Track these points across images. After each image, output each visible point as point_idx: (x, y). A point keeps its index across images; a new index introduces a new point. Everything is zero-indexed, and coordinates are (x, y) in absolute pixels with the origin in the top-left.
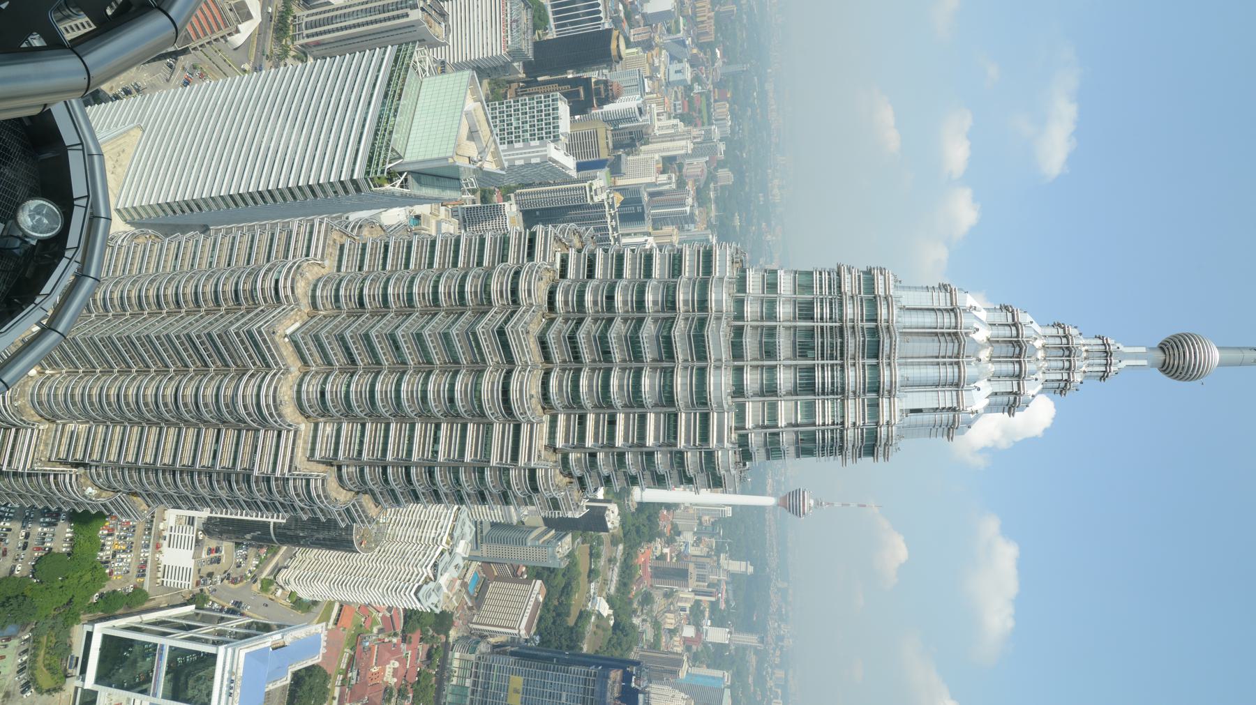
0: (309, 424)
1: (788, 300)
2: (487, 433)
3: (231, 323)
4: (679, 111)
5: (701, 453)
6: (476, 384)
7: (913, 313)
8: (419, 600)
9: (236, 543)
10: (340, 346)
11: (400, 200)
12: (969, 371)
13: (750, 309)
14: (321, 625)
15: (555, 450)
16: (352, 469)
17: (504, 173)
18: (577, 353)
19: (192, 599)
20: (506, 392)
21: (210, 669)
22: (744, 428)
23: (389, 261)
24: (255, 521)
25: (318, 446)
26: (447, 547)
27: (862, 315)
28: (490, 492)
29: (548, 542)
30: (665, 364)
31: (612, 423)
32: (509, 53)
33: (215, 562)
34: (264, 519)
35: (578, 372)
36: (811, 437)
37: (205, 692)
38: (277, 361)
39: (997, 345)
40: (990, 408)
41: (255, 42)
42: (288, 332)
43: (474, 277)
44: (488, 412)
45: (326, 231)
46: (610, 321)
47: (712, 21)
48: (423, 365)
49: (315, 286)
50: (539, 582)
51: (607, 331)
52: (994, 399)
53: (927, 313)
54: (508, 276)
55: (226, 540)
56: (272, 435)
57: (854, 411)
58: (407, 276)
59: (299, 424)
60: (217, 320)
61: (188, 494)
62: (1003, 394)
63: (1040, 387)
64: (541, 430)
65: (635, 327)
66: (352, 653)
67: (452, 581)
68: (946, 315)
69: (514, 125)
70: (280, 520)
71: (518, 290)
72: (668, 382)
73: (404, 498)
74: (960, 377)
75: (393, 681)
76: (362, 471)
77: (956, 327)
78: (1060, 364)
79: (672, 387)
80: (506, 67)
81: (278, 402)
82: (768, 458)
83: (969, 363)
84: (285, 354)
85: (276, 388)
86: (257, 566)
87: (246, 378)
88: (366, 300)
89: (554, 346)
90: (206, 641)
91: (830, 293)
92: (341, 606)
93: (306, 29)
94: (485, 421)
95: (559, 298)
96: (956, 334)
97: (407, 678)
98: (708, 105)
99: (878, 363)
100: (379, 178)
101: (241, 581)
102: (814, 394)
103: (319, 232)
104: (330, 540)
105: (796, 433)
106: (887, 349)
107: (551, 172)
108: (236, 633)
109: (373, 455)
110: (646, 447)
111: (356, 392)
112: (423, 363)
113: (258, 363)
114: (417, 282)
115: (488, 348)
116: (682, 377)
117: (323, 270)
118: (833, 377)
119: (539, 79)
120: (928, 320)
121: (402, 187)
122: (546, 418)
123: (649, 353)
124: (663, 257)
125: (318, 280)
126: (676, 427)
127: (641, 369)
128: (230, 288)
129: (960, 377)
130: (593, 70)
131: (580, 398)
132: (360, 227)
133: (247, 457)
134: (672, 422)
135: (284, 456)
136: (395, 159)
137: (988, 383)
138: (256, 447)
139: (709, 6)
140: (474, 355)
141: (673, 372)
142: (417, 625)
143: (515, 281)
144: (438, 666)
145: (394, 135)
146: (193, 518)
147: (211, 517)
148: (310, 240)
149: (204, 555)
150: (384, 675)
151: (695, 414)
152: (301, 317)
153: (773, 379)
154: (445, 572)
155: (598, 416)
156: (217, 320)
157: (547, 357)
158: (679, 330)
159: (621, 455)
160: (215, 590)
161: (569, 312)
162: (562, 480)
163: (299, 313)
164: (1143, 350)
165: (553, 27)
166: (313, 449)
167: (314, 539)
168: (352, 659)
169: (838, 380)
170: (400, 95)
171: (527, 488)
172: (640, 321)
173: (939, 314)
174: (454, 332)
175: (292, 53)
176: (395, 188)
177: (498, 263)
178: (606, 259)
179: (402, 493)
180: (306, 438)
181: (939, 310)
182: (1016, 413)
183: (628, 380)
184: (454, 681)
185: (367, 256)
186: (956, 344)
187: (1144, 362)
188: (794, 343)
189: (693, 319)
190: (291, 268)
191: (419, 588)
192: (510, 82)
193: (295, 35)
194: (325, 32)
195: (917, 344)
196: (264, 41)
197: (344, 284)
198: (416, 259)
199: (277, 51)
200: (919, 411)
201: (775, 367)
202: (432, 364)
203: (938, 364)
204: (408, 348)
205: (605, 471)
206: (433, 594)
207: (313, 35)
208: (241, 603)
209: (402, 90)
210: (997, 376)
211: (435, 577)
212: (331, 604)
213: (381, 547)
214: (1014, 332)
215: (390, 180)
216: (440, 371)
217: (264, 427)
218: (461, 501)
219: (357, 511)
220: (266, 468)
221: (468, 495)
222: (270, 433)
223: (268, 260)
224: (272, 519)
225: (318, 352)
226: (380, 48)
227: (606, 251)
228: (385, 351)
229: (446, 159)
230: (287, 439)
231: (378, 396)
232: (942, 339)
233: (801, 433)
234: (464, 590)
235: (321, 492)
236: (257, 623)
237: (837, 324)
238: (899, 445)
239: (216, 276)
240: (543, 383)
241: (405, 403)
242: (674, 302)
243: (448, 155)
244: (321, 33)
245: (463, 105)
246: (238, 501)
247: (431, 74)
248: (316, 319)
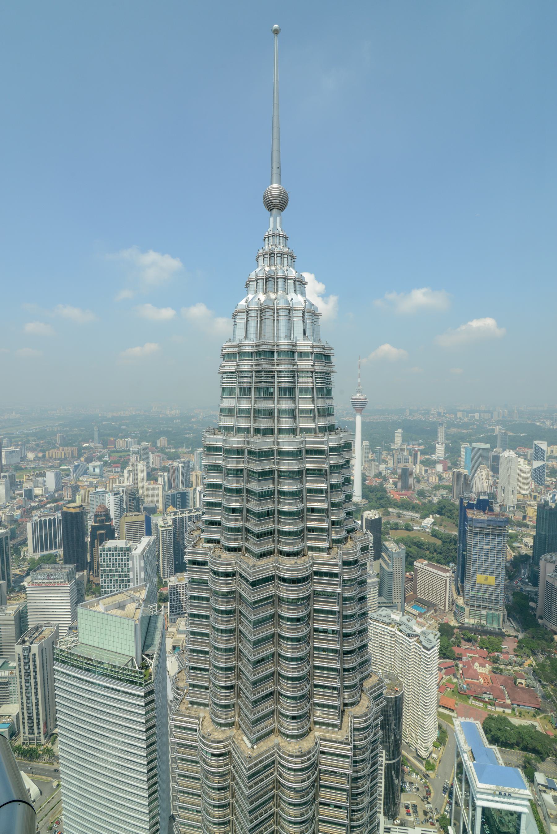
0: (315, 729)
1: (239, 402)
2: (320, 595)
3: (242, 793)
5: (330, 455)
6: (288, 602)
7: (248, 332)
8: (433, 647)
9: (401, 792)
10: (260, 704)
11: (161, 660)
12: (282, 304)
13: (243, 424)
14: (455, 722)
15: (330, 548)
16: (346, 695)
17: (148, 585)
18: (268, 533)
19: (444, 829)
20: (293, 581)
21: (493, 812)
22: (315, 429)
23: (202, 666)
24: (385, 776)
25: (331, 721)
26: (396, 628)
27: (249, 360)
28: (359, 594)
29: (389, 557)
30: (276, 476)
31: (312, 510)
32: (69, 581)
33: (416, 810)
34: (383, 768)
35: (280, 532)
36: (320, 390)
37: (510, 817)
38: (271, 754)
39: (268, 290)
40: (303, 294)
41: (38, 776)
42: (250, 745)
43: (216, 603)
44: (306, 594)
45: (179, 715)
46: (248, 511)
48: (275, 641)
49: (218, 724)
50: (415, 563)
51: (255, 513)
52: (297, 292)
53: (249, 325)
54: (217, 579)
55: (400, 800)
56: (324, 759)
57: (304, 365)
58: (213, 652)
59: (315, 737)
60: (240, 806)
61: (367, 830)
62: (295, 287)
63: (291, 268)
64: (318, 557)
65: (252, 495)
66: (472, 698)
67: (419, 624)
68: (250, 315)
69: (117, 578)
70: (384, 755)
71: (226, 572)
72: (287, 474)
73: (364, 656)
74: (285, 309)
75: (488, 667)
76: (346, 687)
77: (257, 310)
78: (279, 258)
79: (290, 472)
80: (78, 584)
81: (300, 754)
82: (333, 415)
83: (278, 304)
84: (265, 748)
85: (290, 756)
86: (417, 774)
87: (282, 781)
88: (229, 684)
89: (264, 548)
90: (474, 816)
91: (235, 378)
92: (440, 706)
93: (34, 734)
94: (312, 596)
95: (232, 544)
96: (261, 310)
97: (485, 657)
99: (277, 352)
100: (145, 676)
101: (428, 787)
102: (295, 388)
103: (180, 721)
104: (396, 715)
105: (318, 398)
106: (269, 347)
107: (152, 550)
108: (465, 791)
109: (336, 679)
110: (327, 489)
111: (293, 691)
112: (273, 640)
113: (272, 770)
114: (218, 645)
115: (263, 593)
116: (284, 465)
117: (207, 718)
118: (285, 377)
119: (89, 560)
120: (252, 325)
121: (152, 658)
122: (310, 553)
123: (268, 486)
124: (209, 477)
125: (214, 721)
126: (315, 470)
127: (279, 491)
128: (216, 795)
129: (285, 309)
130: (87, 524)
131: (297, 531)
132: (178, 689)
133: (340, 780)
134: (312, 472)
135: (338, 748)
136: (133, 663)
137: (289, 295)
138: (332, 772)
140: (268, 603)
141: (281, 471)
142: (449, 649)
143: (220, 574)
144: (475, 634)
145: (116, 664)
146: (385, 828)
147: (384, 813)
148: (185, 728)
149: (411, 819)
150: (485, 674)
151: (307, 458)
152: (239, 735)
153: (285, 411)
154: (412, 628)
155: (308, 520)
156: (240, 806)
157: (270, 553)
158: (255, 467)
159: (333, 505)
160: (436, 809)
161: (242, 538)
162: (350, 544)
163: (236, 737)
164: (271, 219)
165: (56, 551)
166: (333, 725)
167: (395, 728)
168: (476, 698)
169: (287, 374)
170: (89, 659)
171: (355, 567)
172: (248, 491)
173: (249, 319)
174: (252, 618)
175: (50, 746)
176: (152, 663)
177: (208, 586)
178: (208, 513)
179: (362, 657)
180: (325, 731)
181: (247, 319)
182: (306, 281)
183: (286, 499)
184: (483, 622)
185: (199, 683)
186: (267, 310)
187: (278, 218)
188: (264, 398)
189: (248, 458)
190: (204, 743)
191: (424, 647)
192: (89, 581)
193: (37, 743)
194: (38, 719)
195: (267, 331)
196: (37, 769)
197: (217, 701)
198: (202, 646)
199: (46, 758)
200: (304, 331)
201: (278, 409)
202: (274, 634)
203: (278, 320)
204: (263, 652)
205: (343, 515)
206: (428, 637)
207: (39, 729)
208: (444, 787)
209: (85, 658)
210: (285, 290)
211: (416, 636)
212: (440, 715)
213: (398, 676)
214: (261, 281)
215: (147, 667)
216: (279, 628)
217: (317, 765)
218: (365, 614)
219: (375, 691)
220: (347, 763)
221: (361, 609)
222: (322, 760)
223: (197, 762)
224: (383, 761)
225: (264, 721)
226: (54, 675)
227: (203, 513)
228: (264, 669)
229: (136, 625)
230: (326, 746)
231: (295, 675)
232: (264, 317)
233: (317, 395)
234: (424, 616)
235: (362, 719)
236: (457, 774)
237: (254, 374)
238: (324, 342)
239: (207, 807)
240: (287, 556)
241: (300, 654)
242: (238, 470)
243: (133, 624)
244: (38, 722)
245: (100, 613)
246: (371, 788)
247: (77, 636)
248: (241, 723)
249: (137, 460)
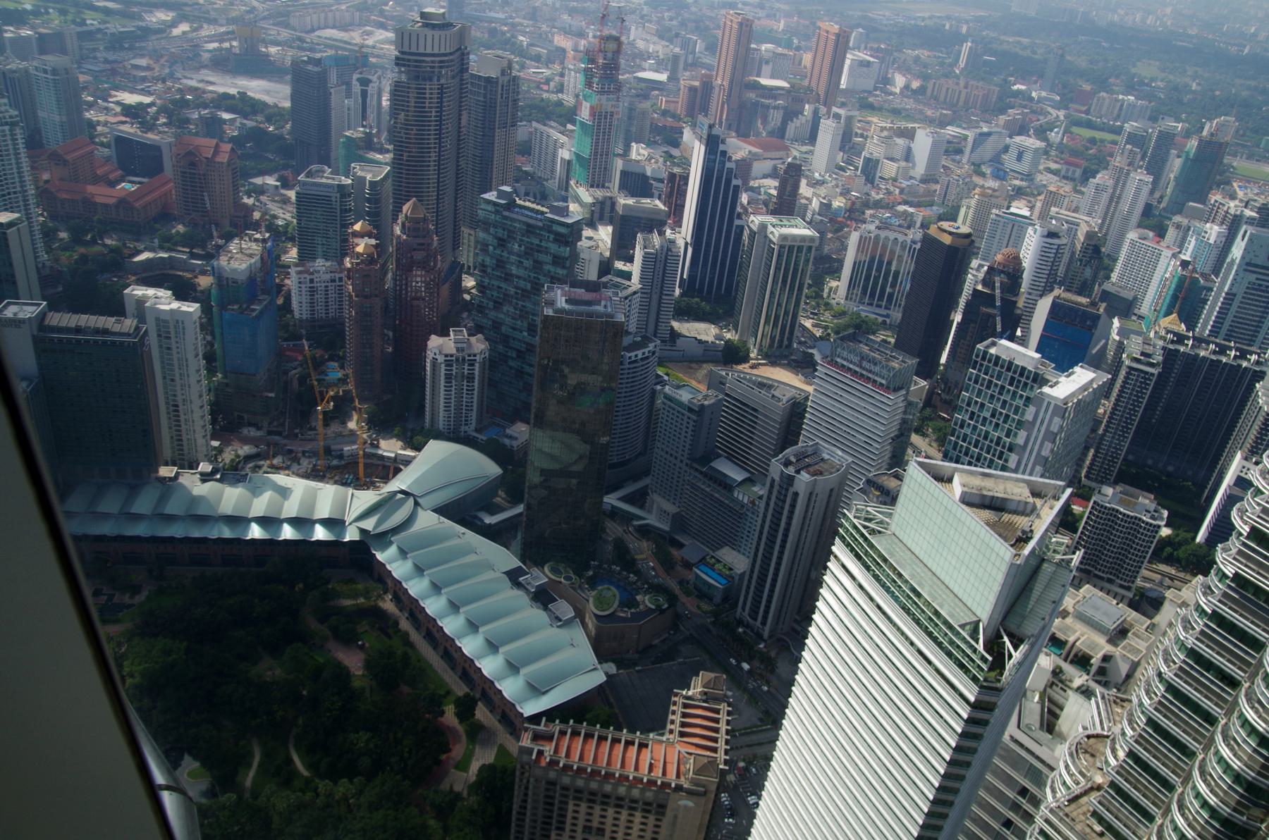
4: (1078, 172)
47: (971, 83)
98: (1090, 125)
139: (950, 82)
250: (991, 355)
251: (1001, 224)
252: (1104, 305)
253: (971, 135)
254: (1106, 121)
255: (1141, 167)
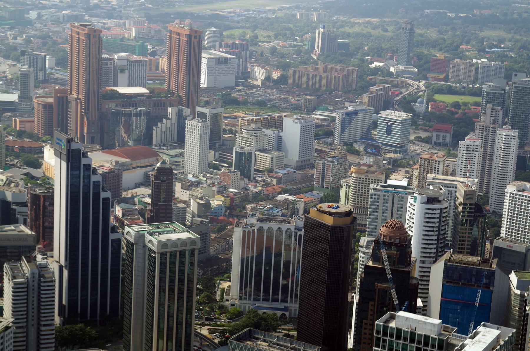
47: (330, 66)
98: (451, 91)
249: (494, 122)
250: (392, 328)
251: (381, 198)
252: (496, 260)
253: (338, 116)
254: (465, 85)
255: (505, 124)
